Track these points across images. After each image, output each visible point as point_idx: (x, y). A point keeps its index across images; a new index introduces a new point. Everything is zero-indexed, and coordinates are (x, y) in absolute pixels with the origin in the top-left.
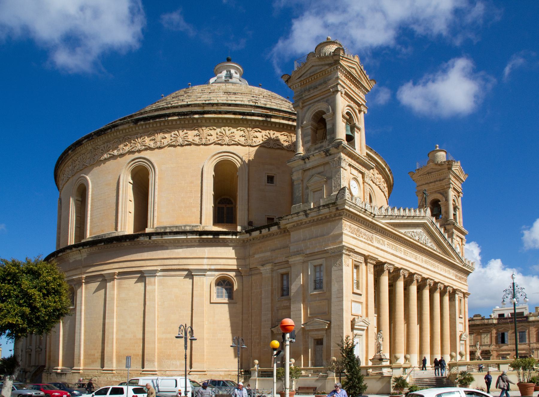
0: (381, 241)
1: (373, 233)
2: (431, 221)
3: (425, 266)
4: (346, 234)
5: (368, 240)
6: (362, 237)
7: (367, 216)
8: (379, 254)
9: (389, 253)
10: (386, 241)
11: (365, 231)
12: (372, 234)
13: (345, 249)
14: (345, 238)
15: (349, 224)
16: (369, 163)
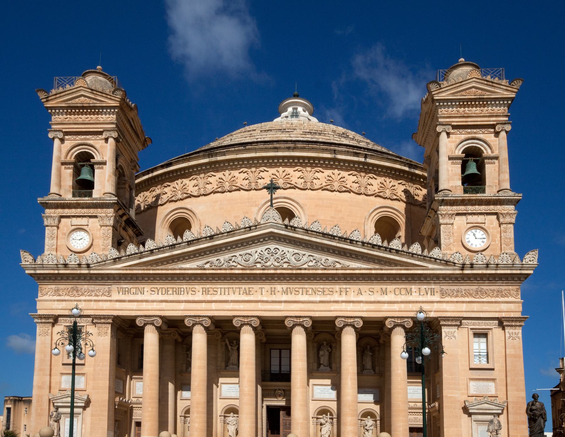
0: (133, 290)
1: (111, 285)
2: (284, 226)
3: (285, 298)
4: (41, 301)
5: (96, 295)
6: (83, 295)
7: (76, 270)
8: (123, 309)
9: (153, 301)
10: (147, 287)
11: (93, 286)
12: (110, 286)
13: (36, 318)
14: (39, 305)
15: (53, 286)
16: (101, 201)
